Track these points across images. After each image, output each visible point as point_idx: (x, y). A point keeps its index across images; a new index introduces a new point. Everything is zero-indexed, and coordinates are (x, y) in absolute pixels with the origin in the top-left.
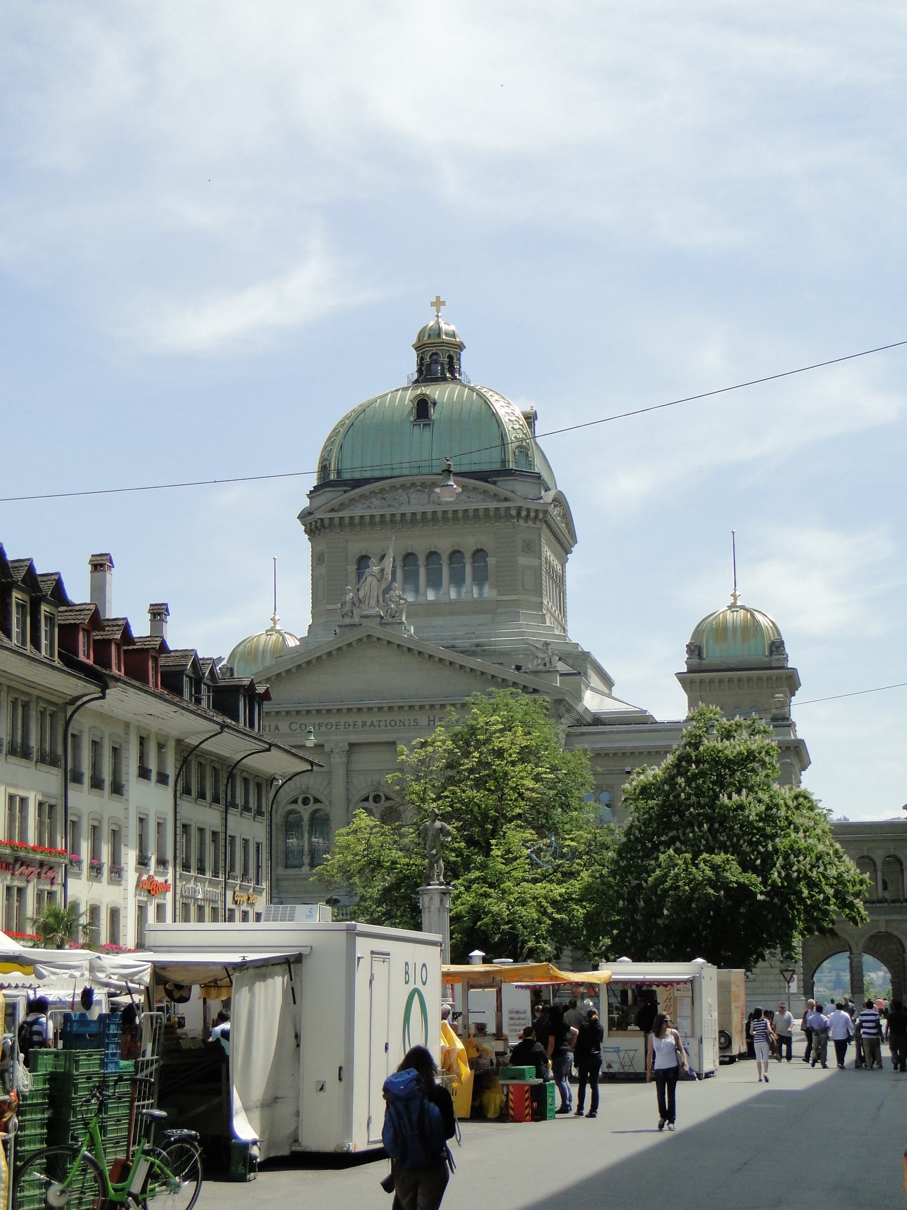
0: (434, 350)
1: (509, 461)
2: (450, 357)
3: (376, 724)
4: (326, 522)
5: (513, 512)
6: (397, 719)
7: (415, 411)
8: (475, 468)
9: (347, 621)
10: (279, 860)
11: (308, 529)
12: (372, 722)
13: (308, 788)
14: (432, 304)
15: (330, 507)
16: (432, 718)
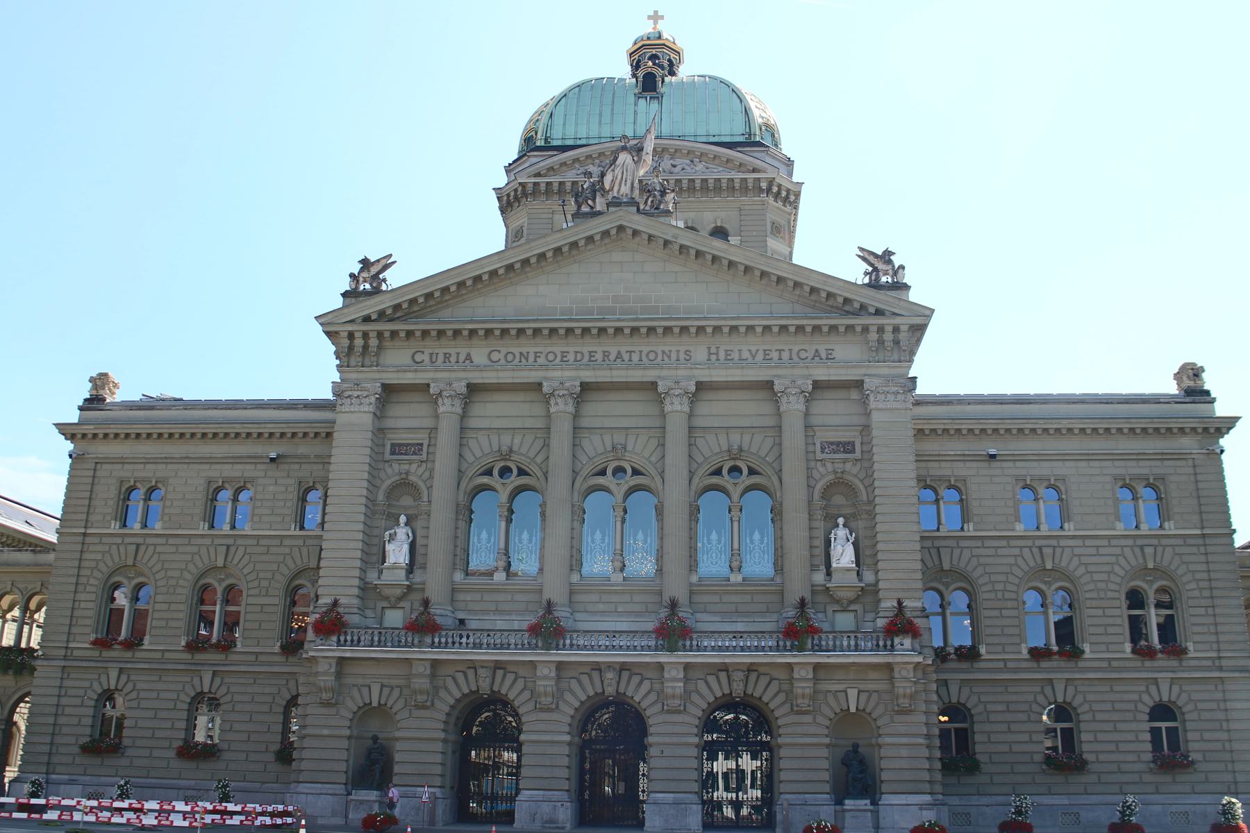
0: (654, 52)
1: (755, 135)
2: (669, 60)
3: (626, 357)
4: (530, 188)
5: (764, 185)
6: (659, 349)
7: (640, 84)
8: (712, 139)
9: (585, 209)
10: (458, 561)
11: (504, 202)
12: (619, 353)
13: (511, 451)
14: (650, 17)
15: (533, 170)
16: (713, 350)
